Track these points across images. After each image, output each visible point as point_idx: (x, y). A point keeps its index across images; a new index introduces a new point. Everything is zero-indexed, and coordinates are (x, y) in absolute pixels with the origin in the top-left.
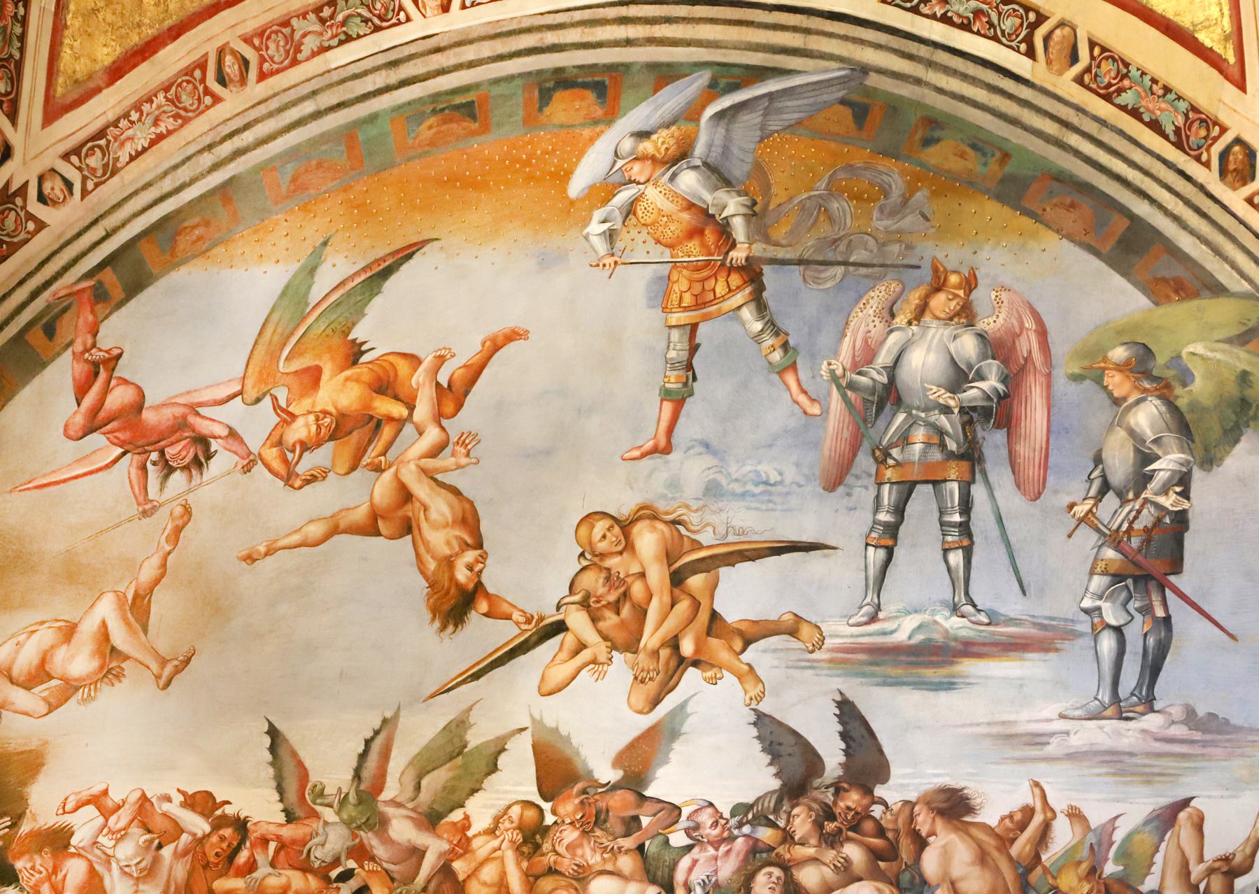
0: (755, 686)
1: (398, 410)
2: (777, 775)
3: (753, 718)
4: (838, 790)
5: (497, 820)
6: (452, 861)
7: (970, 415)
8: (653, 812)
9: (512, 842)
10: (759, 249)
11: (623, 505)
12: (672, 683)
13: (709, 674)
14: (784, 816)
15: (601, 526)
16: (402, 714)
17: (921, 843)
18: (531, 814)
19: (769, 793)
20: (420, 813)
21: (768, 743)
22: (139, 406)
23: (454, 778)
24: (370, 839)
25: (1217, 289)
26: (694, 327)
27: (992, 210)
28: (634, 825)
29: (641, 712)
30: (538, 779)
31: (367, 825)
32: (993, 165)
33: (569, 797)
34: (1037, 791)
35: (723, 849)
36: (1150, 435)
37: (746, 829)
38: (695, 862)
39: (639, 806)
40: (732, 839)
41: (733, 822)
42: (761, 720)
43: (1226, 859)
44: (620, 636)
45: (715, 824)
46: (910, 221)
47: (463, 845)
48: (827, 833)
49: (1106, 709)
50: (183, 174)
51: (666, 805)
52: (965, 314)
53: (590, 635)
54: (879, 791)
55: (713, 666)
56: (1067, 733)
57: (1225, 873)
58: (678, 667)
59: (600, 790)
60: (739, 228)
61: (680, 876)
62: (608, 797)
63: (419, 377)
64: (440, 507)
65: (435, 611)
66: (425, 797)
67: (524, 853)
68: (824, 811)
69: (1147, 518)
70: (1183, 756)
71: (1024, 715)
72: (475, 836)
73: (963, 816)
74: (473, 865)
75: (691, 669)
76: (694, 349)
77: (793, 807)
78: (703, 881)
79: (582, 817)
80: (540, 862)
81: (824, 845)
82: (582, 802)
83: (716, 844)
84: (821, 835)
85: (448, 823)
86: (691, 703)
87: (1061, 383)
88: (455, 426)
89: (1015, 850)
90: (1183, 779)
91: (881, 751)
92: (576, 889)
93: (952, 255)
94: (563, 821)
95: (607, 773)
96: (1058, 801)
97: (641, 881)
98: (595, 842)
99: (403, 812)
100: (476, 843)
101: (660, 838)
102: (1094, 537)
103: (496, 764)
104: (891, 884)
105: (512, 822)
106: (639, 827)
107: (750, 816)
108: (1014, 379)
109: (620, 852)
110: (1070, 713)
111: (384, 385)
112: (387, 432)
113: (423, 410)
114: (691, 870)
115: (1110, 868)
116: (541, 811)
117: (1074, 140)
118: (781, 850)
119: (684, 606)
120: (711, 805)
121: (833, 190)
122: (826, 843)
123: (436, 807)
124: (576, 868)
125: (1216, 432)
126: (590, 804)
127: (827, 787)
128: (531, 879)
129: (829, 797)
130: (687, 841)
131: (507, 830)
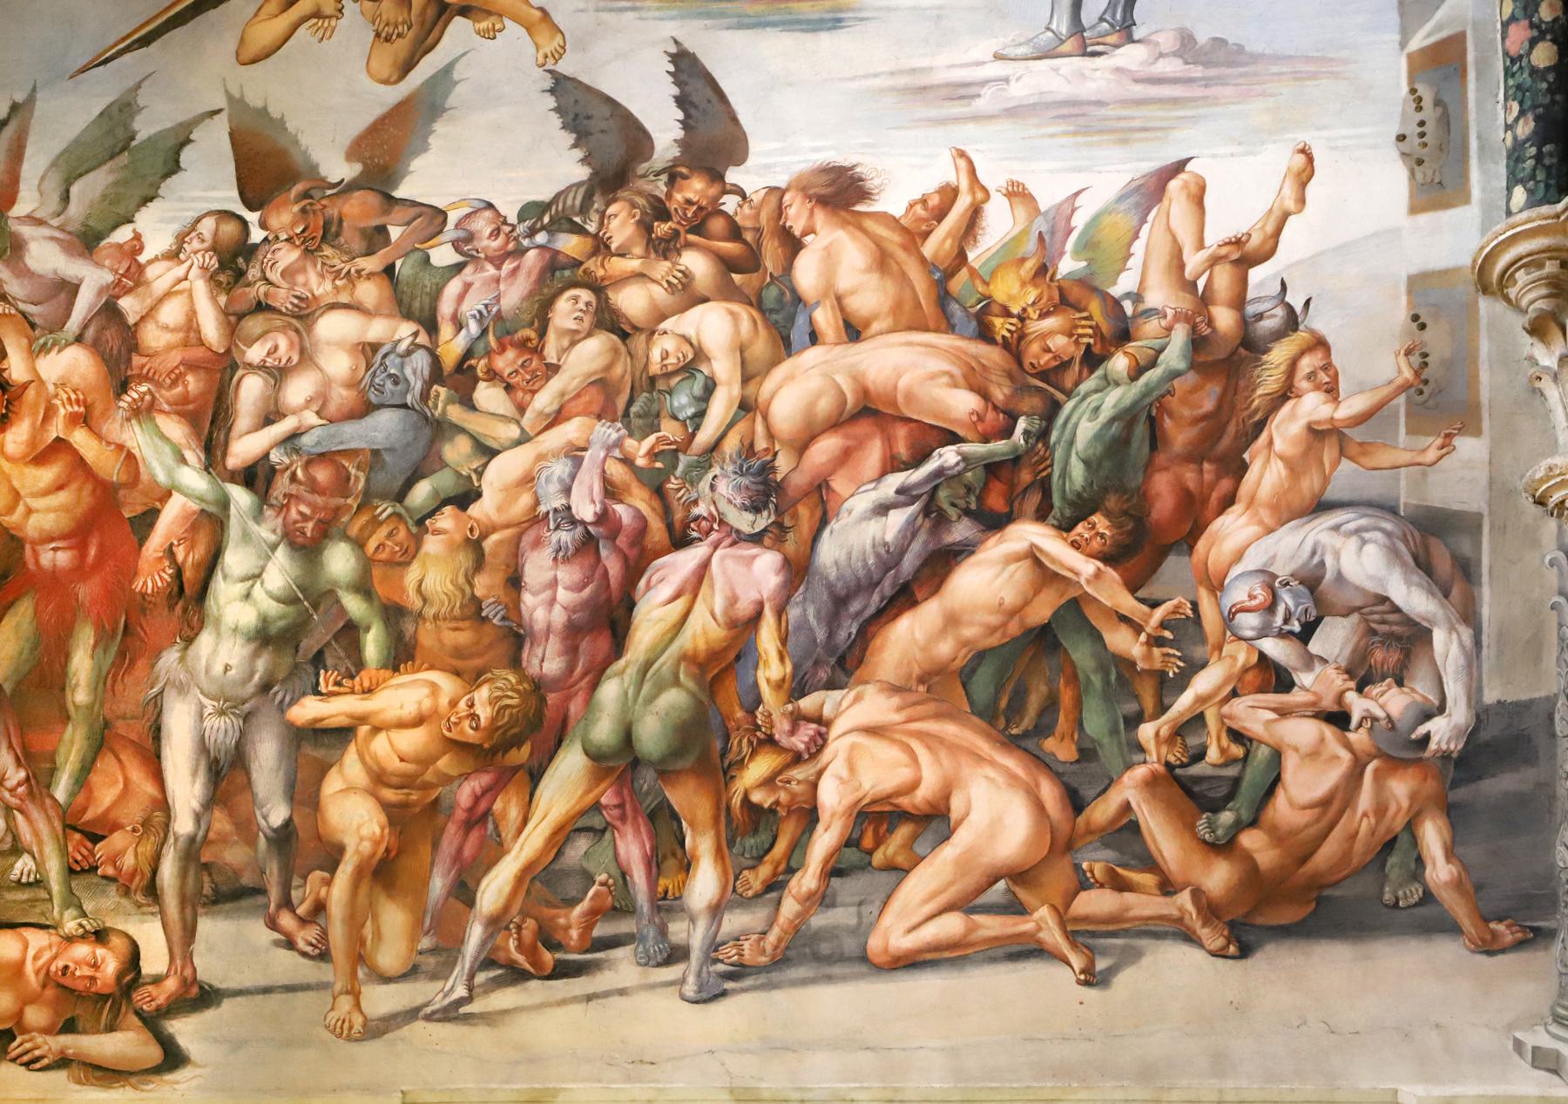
0: (552, 38)
2: (584, 161)
3: (548, 83)
4: (673, 176)
5: (181, 239)
6: (118, 297)
8: (406, 220)
9: (203, 268)
12: (430, 40)
13: (484, 25)
14: (595, 217)
16: (39, 95)
17: (793, 245)
18: (229, 229)
19: (573, 186)
20: (70, 233)
21: (571, 117)
23: (116, 183)
28: (380, 238)
29: (386, 82)
30: (239, 180)
33: (286, 203)
34: (962, 163)
35: (508, 266)
37: (541, 238)
38: (467, 286)
39: (386, 212)
40: (520, 252)
41: (521, 228)
42: (561, 86)
43: (1238, 242)
45: (496, 233)
47: (133, 275)
48: (658, 238)
49: (1063, 42)
51: (424, 209)
54: (733, 176)
55: (489, 13)
56: (1006, 80)
57: (1236, 262)
58: (439, 16)
59: (329, 192)
61: (446, 307)
62: (339, 202)
66: (76, 209)
67: (221, 283)
68: (653, 208)
70: (1175, 101)
71: (942, 60)
72: (150, 262)
73: (854, 204)
74: (149, 302)
75: (458, 20)
77: (608, 205)
78: (480, 312)
79: (303, 231)
80: (245, 294)
81: (653, 255)
82: (303, 211)
83: (498, 262)
84: (649, 241)
85: (111, 245)
86: (458, 67)
89: (929, 248)
90: (1176, 134)
91: (735, 120)
92: (297, 331)
94: (277, 238)
95: (339, 169)
96: (993, 176)
97: (390, 316)
98: (323, 264)
99: (46, 231)
100: (151, 272)
101: (417, 256)
103: (177, 162)
104: (751, 304)
105: (203, 241)
106: (387, 241)
107: (546, 219)
109: (360, 276)
110: (1011, 52)
114: (461, 298)
115: (1068, 265)
116: (244, 224)
118: (591, 264)
120: (490, 206)
122: (656, 252)
123: (91, 223)
124: (296, 301)
126: (314, 212)
127: (657, 174)
128: (233, 319)
129: (661, 188)
130: (457, 258)
131: (196, 253)
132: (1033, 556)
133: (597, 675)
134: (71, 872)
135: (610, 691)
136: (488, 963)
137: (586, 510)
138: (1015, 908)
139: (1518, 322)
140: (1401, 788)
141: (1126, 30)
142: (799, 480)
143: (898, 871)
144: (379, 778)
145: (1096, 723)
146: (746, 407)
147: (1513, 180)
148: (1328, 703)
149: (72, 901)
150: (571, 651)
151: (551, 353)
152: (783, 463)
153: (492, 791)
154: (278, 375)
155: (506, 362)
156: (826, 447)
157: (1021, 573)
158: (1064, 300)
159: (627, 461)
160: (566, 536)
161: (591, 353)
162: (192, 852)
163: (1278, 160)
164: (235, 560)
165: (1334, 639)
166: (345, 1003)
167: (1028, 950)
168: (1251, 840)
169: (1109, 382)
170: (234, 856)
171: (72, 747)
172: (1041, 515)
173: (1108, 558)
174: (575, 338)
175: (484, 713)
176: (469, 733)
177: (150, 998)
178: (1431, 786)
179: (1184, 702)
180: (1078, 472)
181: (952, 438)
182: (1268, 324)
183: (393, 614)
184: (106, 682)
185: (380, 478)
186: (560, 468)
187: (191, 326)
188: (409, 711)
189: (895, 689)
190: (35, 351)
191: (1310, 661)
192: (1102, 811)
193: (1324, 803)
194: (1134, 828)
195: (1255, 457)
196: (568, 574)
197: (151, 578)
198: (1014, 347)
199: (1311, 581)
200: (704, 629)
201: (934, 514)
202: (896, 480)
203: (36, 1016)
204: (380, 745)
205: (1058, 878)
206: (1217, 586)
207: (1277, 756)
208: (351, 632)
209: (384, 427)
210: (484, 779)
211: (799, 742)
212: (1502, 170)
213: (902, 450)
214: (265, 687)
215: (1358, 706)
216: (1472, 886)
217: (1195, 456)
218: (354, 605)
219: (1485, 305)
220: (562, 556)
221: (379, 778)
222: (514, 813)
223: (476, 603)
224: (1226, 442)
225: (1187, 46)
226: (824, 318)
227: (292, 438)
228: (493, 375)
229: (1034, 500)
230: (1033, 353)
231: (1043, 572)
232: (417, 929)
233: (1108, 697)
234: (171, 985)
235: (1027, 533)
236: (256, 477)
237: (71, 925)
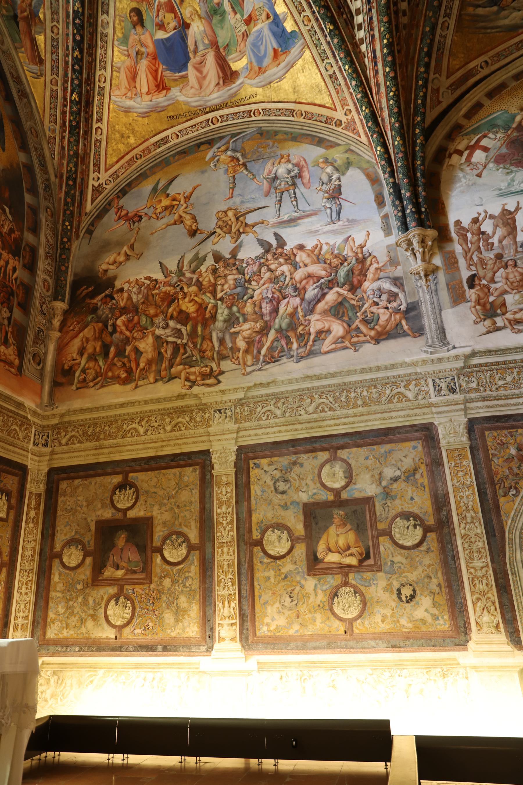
1: (177, 203)
4: (276, 249)
7: (292, 178)
10: (245, 160)
11: (224, 208)
15: (220, 213)
17: (295, 255)
18: (214, 267)
22: (128, 213)
24: (182, 278)
25: (339, 145)
26: (234, 176)
27: (290, 143)
31: (181, 276)
32: (290, 136)
36: (330, 172)
42: (258, 240)
44: (227, 231)
46: (274, 149)
47: (201, 275)
50: (132, 175)
52: (289, 161)
53: (220, 232)
54: (285, 248)
60: (240, 158)
61: (246, 272)
63: (181, 196)
64: (188, 217)
65: (189, 235)
66: (192, 268)
69: (333, 187)
76: (234, 179)
83: (252, 265)
87: (310, 168)
88: (188, 203)
89: (315, 253)
93: (284, 152)
95: (228, 256)
96: (323, 242)
102: (322, 193)
108: (301, 169)
111: (174, 199)
112: (176, 207)
113: (182, 202)
117: (305, 128)
119: (239, 223)
121: (258, 148)
125: (344, 169)
129: (275, 251)
132: (337, 292)
133: (275, 319)
134: (201, 358)
135: (277, 321)
136: (264, 362)
137: (270, 296)
138: (343, 342)
139: (403, 250)
140: (398, 316)
141: (339, 220)
142: (301, 287)
143: (324, 339)
144: (244, 338)
145: (350, 314)
146: (291, 278)
147: (399, 231)
148: (385, 306)
149: (202, 362)
150: (270, 316)
151: (262, 276)
152: (298, 285)
153: (261, 337)
154: (223, 285)
155: (255, 278)
156: (304, 282)
157: (336, 295)
158: (336, 257)
159: (275, 288)
160: (267, 300)
161: (268, 275)
162: (218, 353)
163: (364, 233)
164: (220, 311)
165: (384, 297)
166: (243, 371)
167: (346, 348)
168: (377, 327)
169: (345, 267)
170: (225, 352)
171: (199, 340)
172: (338, 286)
173: (349, 291)
174: (265, 273)
175: (259, 327)
176: (257, 330)
177: (215, 374)
178: (402, 316)
179: (363, 309)
180: (342, 280)
181: (323, 278)
182: (366, 256)
183: (243, 315)
184: (202, 331)
185: (239, 297)
186: (265, 291)
187: (210, 281)
188: (248, 328)
189: (320, 314)
190: (188, 287)
191: (381, 301)
192: (353, 326)
193: (387, 320)
194: (359, 328)
195: (368, 273)
196: (268, 305)
197: (208, 315)
198: (330, 264)
199: (379, 290)
200: (290, 310)
201: (321, 288)
202: (315, 285)
203: (198, 379)
204: (244, 333)
205: (348, 337)
206: (365, 292)
207: (378, 315)
208: (238, 318)
209: (239, 289)
210: (260, 336)
211: (306, 323)
212: (397, 230)
213: (316, 281)
214: (226, 328)
215: (389, 306)
216: (411, 329)
217: (359, 275)
218: (238, 315)
219: (398, 248)
220: (267, 303)
221: (244, 338)
222: (265, 340)
223: (255, 312)
224: (363, 272)
225: (348, 220)
226: (301, 264)
227: (226, 294)
228: (254, 280)
229: (336, 284)
230: (333, 264)
231: (339, 294)
232: (253, 358)
233: (352, 310)
234: (218, 372)
235: (336, 289)
236: (221, 299)
237: (202, 365)
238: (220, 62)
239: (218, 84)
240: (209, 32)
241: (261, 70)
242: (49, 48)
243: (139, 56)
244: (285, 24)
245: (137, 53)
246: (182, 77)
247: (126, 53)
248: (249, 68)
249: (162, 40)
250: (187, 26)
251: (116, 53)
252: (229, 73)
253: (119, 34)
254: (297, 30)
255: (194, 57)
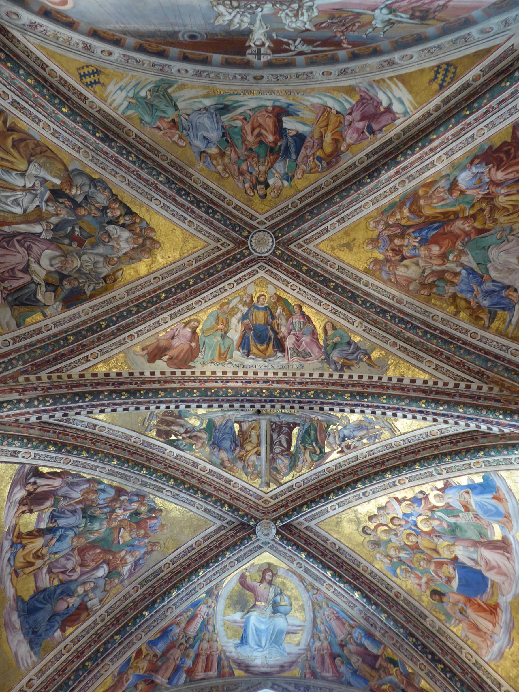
238: (491, 547)
239: (508, 558)
240: (465, 543)
241: (507, 516)
242: (431, 682)
243: (464, 612)
244: (476, 482)
245: (461, 613)
246: (492, 586)
247: (457, 622)
248: (503, 525)
249: (459, 585)
250: (456, 558)
251: (455, 630)
252: (502, 544)
253: (443, 618)
254: (483, 474)
255: (481, 566)
